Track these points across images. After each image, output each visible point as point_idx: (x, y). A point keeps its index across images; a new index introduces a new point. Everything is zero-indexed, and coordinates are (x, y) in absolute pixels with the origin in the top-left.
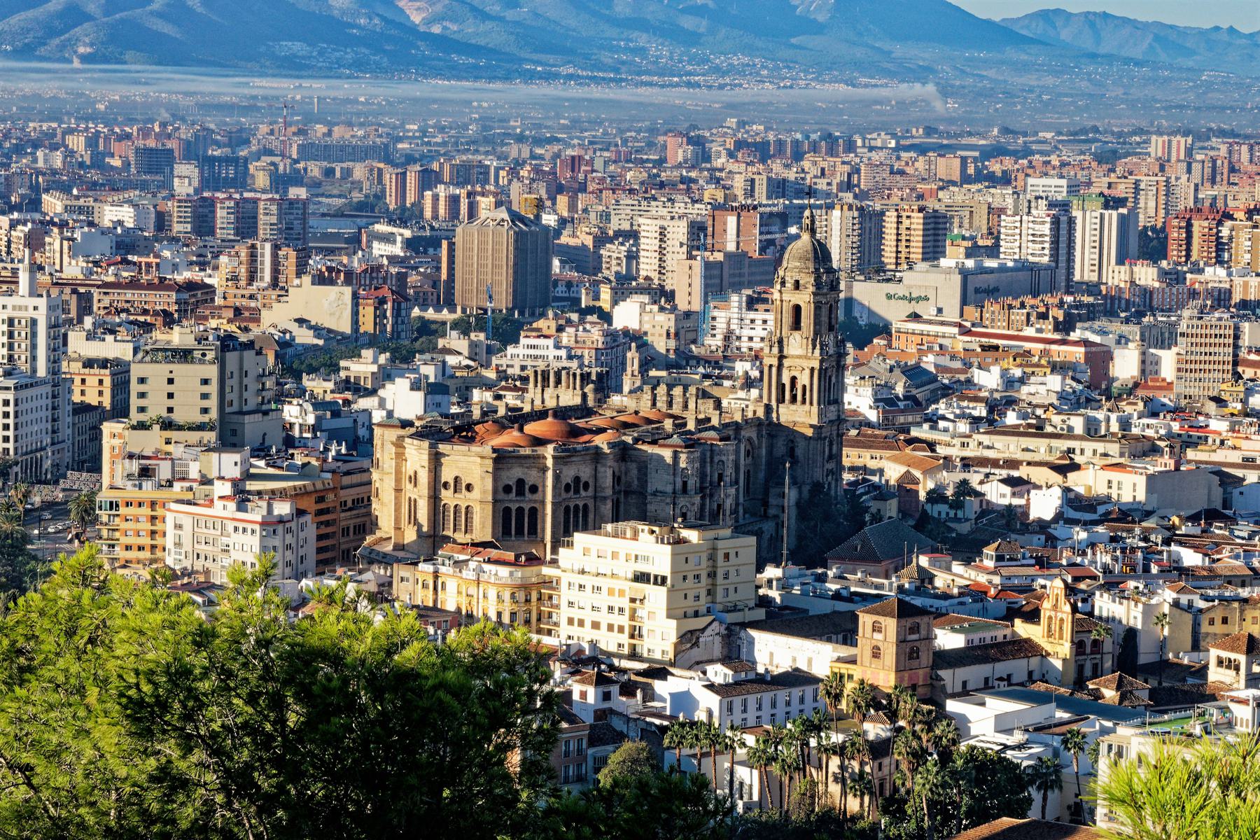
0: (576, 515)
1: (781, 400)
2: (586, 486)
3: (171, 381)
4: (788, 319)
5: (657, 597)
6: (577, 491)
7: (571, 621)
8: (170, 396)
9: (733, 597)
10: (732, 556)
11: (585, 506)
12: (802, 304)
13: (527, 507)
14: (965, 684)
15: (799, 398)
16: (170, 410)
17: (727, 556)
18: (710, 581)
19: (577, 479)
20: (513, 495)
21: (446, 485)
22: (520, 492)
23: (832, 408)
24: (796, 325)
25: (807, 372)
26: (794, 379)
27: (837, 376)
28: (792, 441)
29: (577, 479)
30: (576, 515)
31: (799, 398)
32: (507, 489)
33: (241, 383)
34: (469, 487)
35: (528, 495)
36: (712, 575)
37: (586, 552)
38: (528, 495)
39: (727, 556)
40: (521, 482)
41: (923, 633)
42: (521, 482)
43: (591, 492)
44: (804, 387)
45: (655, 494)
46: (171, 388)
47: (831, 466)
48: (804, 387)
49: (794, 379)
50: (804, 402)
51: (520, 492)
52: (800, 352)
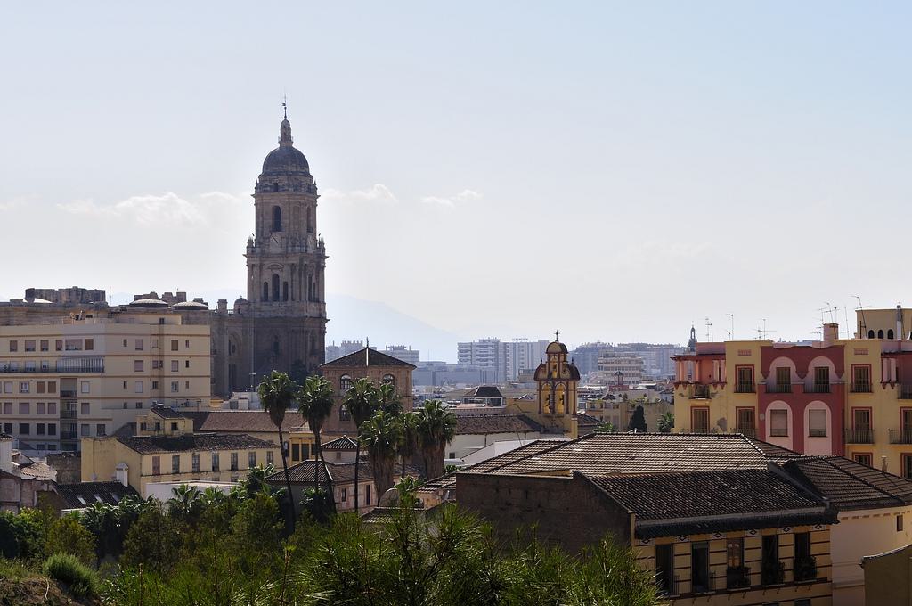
1: (265, 299)
4: (269, 221)
9: (182, 391)
10: (181, 345)
12: (280, 205)
15: (281, 294)
17: (175, 345)
23: (313, 305)
24: (277, 227)
25: (287, 268)
26: (276, 278)
27: (317, 277)
28: (276, 337)
31: (281, 294)
36: (159, 365)
39: (175, 345)
44: (286, 284)
48: (286, 284)
49: (276, 278)
50: (286, 299)
52: (280, 250)
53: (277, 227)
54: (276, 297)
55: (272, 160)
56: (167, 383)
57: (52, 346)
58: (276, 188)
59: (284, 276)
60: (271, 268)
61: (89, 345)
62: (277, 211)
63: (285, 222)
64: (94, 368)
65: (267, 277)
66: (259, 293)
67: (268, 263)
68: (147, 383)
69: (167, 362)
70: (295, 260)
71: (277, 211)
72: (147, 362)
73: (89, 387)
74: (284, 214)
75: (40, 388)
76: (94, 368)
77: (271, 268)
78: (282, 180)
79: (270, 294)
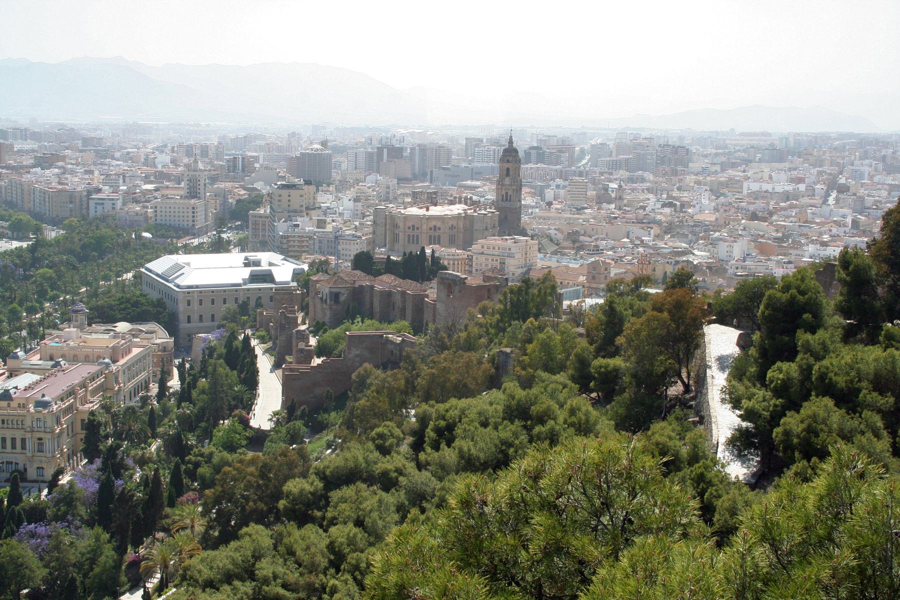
1: (502, 200)
3: (289, 196)
4: (505, 173)
7: (477, 270)
8: (289, 201)
9: (531, 261)
13: (437, 235)
16: (289, 206)
21: (409, 228)
22: (435, 230)
24: (508, 175)
26: (507, 193)
32: (431, 229)
34: (418, 229)
36: (526, 254)
37: (483, 247)
40: (435, 227)
42: (435, 227)
45: (477, 230)
46: (289, 198)
49: (507, 193)
50: (510, 201)
51: (435, 230)
53: (508, 175)
54: (507, 200)
55: (505, 151)
57: (497, 248)
58: (508, 161)
59: (510, 193)
61: (510, 249)
62: (508, 169)
63: (511, 173)
64: (511, 256)
65: (504, 193)
66: (500, 198)
67: (504, 188)
70: (514, 187)
71: (508, 169)
73: (509, 261)
74: (511, 171)
75: (493, 260)
76: (511, 256)
78: (511, 159)
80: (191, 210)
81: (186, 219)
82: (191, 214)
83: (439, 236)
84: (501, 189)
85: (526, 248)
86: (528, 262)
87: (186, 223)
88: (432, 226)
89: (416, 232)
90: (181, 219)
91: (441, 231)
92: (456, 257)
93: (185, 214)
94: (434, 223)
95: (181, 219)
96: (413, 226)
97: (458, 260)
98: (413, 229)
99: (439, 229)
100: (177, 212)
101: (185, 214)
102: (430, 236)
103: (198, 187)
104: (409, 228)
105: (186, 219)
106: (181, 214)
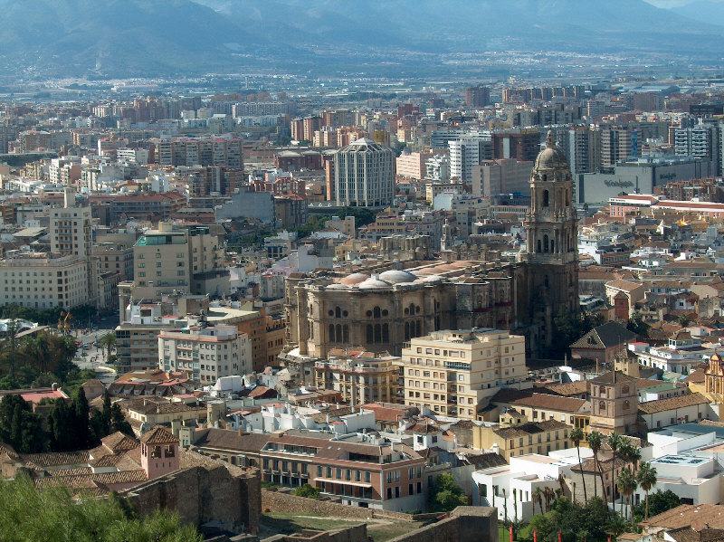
0: (339, 333)
1: (539, 251)
2: (418, 309)
5: (464, 378)
6: (412, 313)
7: (411, 394)
8: (159, 265)
9: (511, 374)
10: (510, 349)
11: (418, 321)
13: (382, 324)
14: (659, 423)
18: (497, 365)
19: (412, 305)
20: (372, 317)
23: (571, 254)
29: (412, 305)
30: (339, 333)
32: (369, 313)
33: (202, 255)
35: (383, 318)
36: (498, 362)
37: (419, 350)
38: (383, 318)
40: (377, 309)
41: (631, 392)
42: (377, 309)
43: (421, 313)
47: (571, 290)
56: (503, 371)
60: (543, 231)
65: (540, 237)
67: (541, 227)
68: (493, 372)
69: (503, 360)
72: (493, 361)
77: (543, 231)
79: (542, 248)
80: (55, 278)
81: (47, 293)
82: (55, 285)
83: (386, 326)
84: (536, 230)
85: (498, 350)
86: (503, 375)
87: (47, 300)
88: (372, 309)
89: (342, 321)
90: (40, 293)
91: (389, 317)
92: (380, 369)
93: (47, 285)
94: (370, 304)
95: (40, 293)
96: (338, 310)
97: (384, 374)
98: (338, 315)
99: (386, 313)
100: (24, 282)
101: (47, 285)
102: (369, 326)
103: (74, 235)
104: (331, 313)
105: (47, 293)
106: (39, 285)
